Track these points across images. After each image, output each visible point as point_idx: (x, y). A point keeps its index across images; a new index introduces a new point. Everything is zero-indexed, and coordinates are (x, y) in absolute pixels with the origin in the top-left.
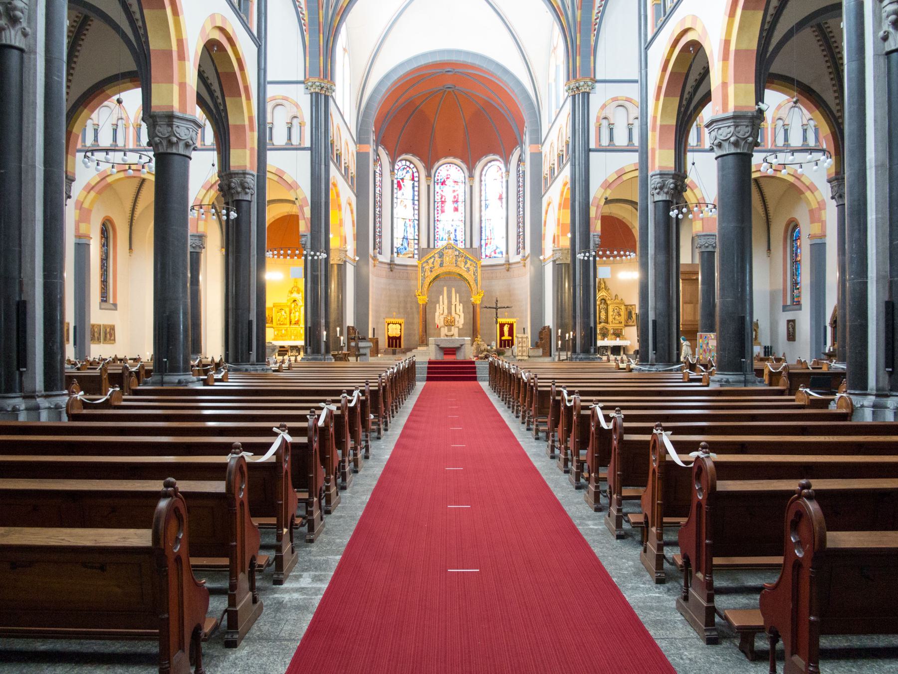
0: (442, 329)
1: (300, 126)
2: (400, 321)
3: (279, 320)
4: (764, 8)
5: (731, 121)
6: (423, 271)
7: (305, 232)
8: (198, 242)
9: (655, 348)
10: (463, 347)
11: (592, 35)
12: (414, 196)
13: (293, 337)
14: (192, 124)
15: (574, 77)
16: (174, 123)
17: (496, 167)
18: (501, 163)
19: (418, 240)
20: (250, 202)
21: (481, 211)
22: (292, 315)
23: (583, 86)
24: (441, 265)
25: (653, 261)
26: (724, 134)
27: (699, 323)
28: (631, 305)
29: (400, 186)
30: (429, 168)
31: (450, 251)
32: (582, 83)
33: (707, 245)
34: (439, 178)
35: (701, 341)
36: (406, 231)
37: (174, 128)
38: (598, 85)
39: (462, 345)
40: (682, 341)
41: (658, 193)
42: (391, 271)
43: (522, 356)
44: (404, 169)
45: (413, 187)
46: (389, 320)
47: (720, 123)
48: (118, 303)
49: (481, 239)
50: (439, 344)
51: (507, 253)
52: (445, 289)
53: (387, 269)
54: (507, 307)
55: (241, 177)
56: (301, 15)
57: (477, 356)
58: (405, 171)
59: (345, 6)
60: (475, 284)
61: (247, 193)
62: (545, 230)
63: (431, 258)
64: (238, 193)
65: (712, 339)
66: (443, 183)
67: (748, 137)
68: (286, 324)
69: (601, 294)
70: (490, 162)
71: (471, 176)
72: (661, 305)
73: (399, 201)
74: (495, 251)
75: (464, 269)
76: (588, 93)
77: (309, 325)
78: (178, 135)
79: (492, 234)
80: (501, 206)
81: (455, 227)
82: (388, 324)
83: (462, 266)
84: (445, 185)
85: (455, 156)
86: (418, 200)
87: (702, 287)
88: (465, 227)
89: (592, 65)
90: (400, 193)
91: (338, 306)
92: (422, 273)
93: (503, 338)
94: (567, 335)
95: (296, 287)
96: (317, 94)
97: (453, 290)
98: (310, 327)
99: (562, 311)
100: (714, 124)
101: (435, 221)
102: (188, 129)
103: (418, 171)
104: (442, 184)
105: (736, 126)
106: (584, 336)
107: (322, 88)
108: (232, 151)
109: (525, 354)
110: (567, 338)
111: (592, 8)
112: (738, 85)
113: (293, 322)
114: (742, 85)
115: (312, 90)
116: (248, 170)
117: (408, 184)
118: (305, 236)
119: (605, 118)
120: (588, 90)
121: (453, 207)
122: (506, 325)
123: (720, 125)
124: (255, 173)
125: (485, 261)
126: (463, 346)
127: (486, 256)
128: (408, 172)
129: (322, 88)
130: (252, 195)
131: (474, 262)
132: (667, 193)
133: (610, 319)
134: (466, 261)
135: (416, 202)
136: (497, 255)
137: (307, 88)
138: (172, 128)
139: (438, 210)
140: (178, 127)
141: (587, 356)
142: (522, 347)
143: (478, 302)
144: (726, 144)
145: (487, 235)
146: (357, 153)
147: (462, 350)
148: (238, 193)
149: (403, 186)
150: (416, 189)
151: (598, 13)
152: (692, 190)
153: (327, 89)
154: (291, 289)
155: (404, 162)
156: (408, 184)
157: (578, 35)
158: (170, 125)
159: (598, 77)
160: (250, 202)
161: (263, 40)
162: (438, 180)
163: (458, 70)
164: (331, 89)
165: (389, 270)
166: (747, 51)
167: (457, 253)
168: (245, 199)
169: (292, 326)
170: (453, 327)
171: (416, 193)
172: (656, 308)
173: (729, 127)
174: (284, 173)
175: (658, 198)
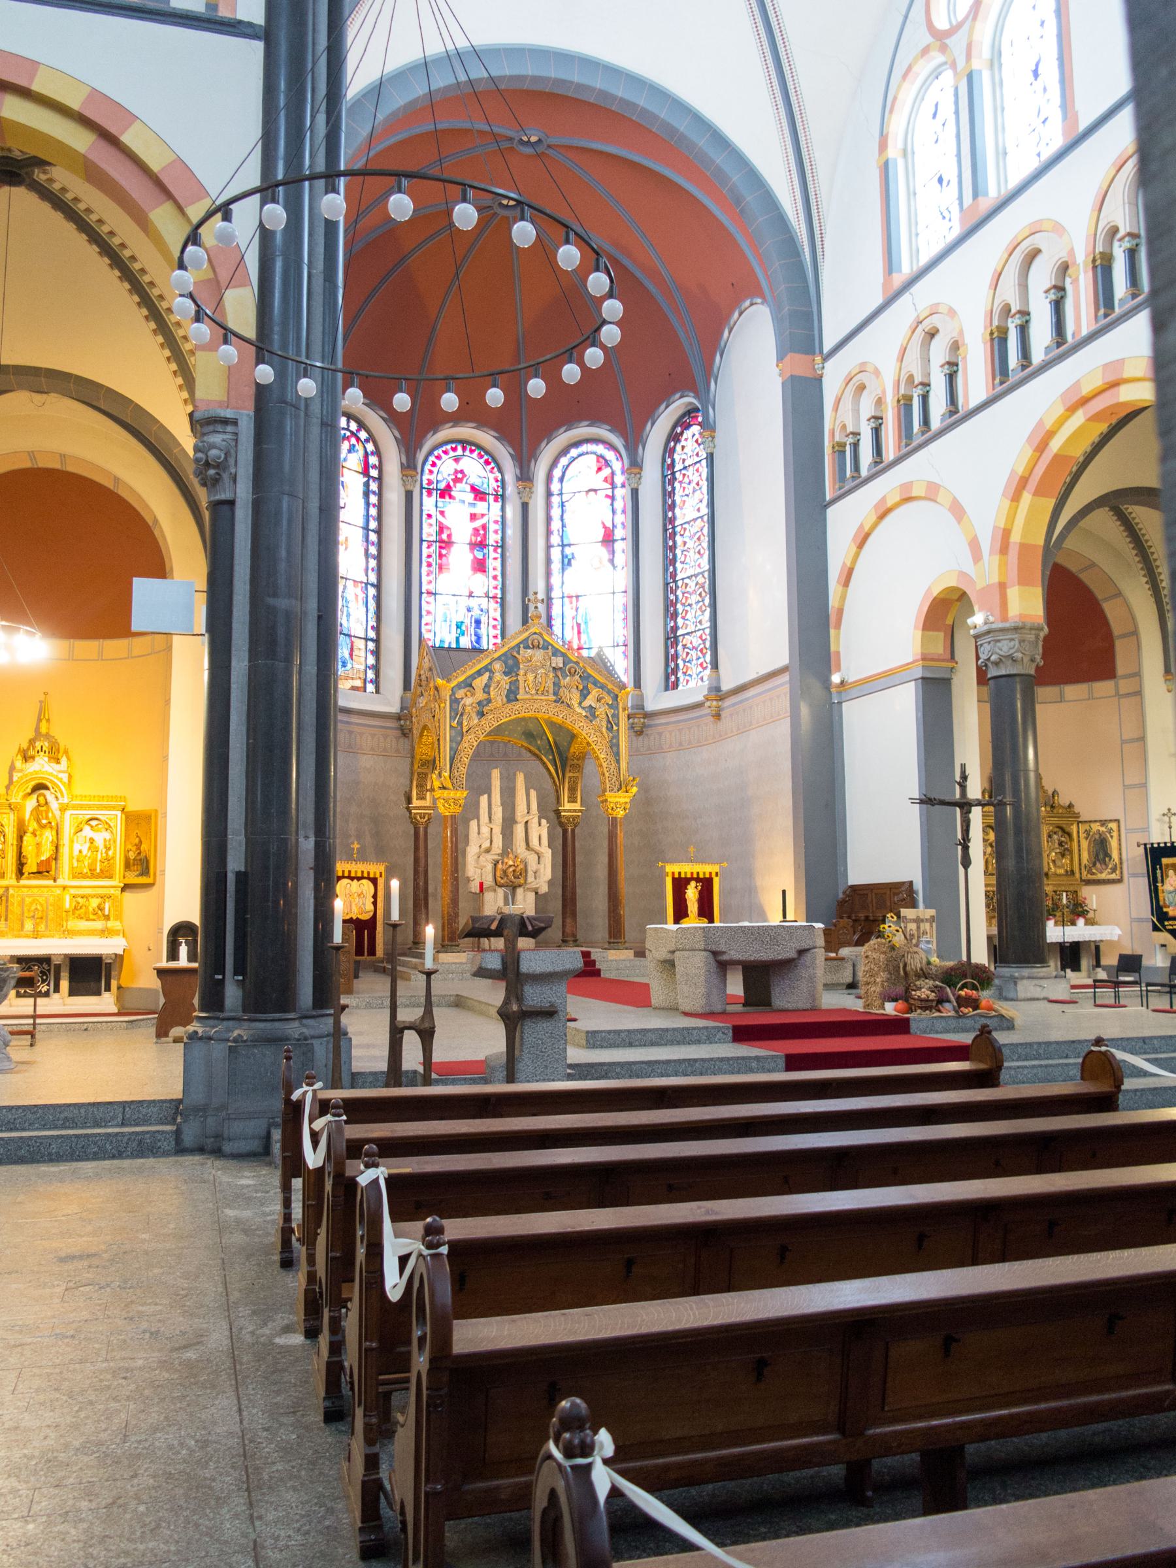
12: (367, 517)
13: (29, 926)
17: (594, 457)
18: (611, 446)
19: (377, 641)
21: (548, 574)
22: (28, 838)
24: (512, 695)
28: (1103, 823)
31: (538, 655)
39: (802, 952)
45: (366, 494)
50: (722, 948)
52: (496, 774)
60: (611, 758)
62: (843, 598)
63: (479, 673)
66: (446, 493)
70: (577, 444)
75: (579, 710)
77: (235, 862)
79: (583, 636)
80: (612, 561)
81: (476, 613)
84: (451, 497)
86: (379, 532)
88: (503, 615)
92: (452, 718)
95: (47, 736)
97: (520, 780)
98: (238, 874)
101: (421, 593)
104: (442, 496)
118: (225, 422)
121: (471, 557)
122: (693, 883)
126: (808, 957)
135: (373, 537)
143: (621, 813)
154: (25, 745)
162: (430, 482)
167: (558, 662)
169: (23, 882)
171: (373, 511)
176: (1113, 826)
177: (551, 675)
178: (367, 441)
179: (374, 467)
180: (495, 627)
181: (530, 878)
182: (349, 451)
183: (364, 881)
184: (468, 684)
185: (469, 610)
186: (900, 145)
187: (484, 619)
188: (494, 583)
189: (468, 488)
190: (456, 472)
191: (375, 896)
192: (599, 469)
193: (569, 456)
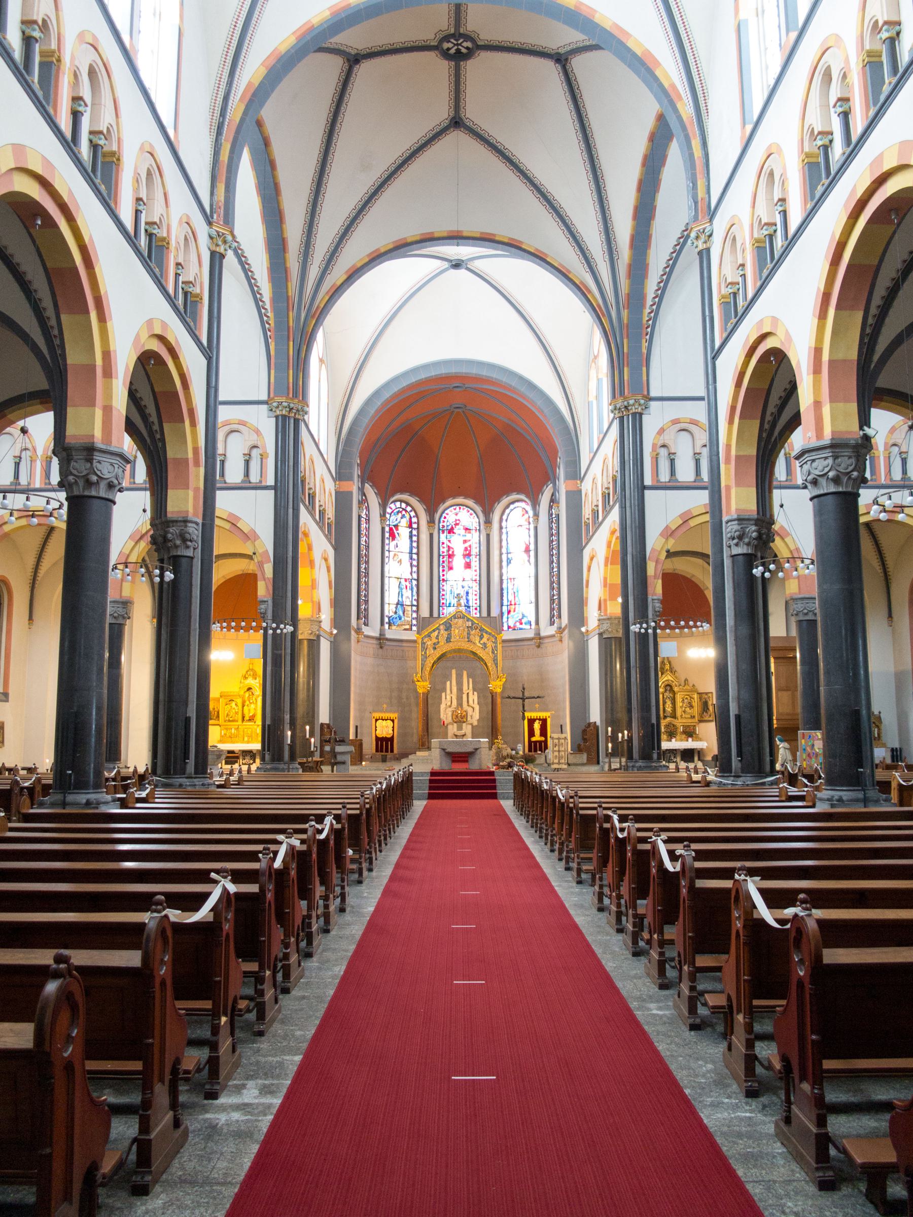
0: (450, 727)
1: (262, 459)
2: (393, 716)
3: (228, 715)
4: (863, 308)
5: (828, 451)
6: (424, 648)
7: (265, 596)
8: (121, 611)
9: (740, 753)
10: (478, 751)
11: (644, 341)
12: (411, 548)
13: (246, 739)
14: (118, 459)
15: (622, 393)
16: (95, 457)
18: (528, 504)
19: (418, 606)
20: (192, 558)
21: (501, 567)
22: (245, 708)
23: (634, 405)
24: (448, 640)
25: (733, 634)
26: (820, 468)
27: (800, 717)
28: (707, 694)
29: (393, 536)
30: (431, 511)
31: (460, 621)
32: (631, 402)
33: (806, 611)
34: (445, 524)
35: (803, 741)
36: (400, 594)
37: (95, 464)
38: (653, 404)
39: (476, 749)
40: (778, 743)
41: (737, 545)
42: (381, 647)
43: (559, 763)
44: (398, 512)
45: (411, 537)
46: (377, 715)
47: (814, 453)
48: (11, 691)
49: (502, 605)
50: (445, 747)
51: (537, 623)
52: (454, 672)
53: (375, 646)
54: (538, 697)
55: (182, 526)
56: (265, 318)
57: (498, 765)
58: (400, 515)
59: (322, 306)
60: (494, 666)
61: (188, 547)
62: (587, 593)
63: (434, 631)
64: (176, 547)
65: (819, 739)
66: (451, 531)
67: (852, 471)
68: (237, 721)
69: (666, 678)
70: (513, 503)
71: (488, 522)
72: (746, 695)
73: (392, 554)
74: (521, 620)
76: (641, 414)
77: (268, 722)
78: (99, 473)
80: (529, 561)
81: (466, 589)
82: (376, 720)
83: (477, 642)
84: (453, 533)
85: (466, 496)
86: (418, 554)
87: (801, 669)
88: (480, 589)
89: (645, 378)
90: (393, 544)
91: (308, 696)
92: (422, 651)
93: (533, 739)
94: (620, 735)
95: (252, 670)
96: (284, 417)
97: (465, 673)
99: (612, 702)
100: (806, 456)
101: (439, 581)
102: (112, 464)
103: (417, 516)
104: (449, 533)
105: (835, 457)
106: (643, 736)
107: (291, 409)
108: (170, 492)
109: (563, 761)
110: (620, 740)
111: (642, 305)
112: (834, 405)
113: (247, 718)
114: (841, 405)
115: (278, 413)
116: (191, 517)
117: (404, 532)
118: (265, 601)
119: (664, 446)
120: (640, 410)
121: (464, 561)
122: (537, 721)
123: (814, 456)
124: (200, 521)
125: (507, 635)
126: (478, 751)
127: (509, 627)
128: (403, 517)
129: (291, 409)
130: (194, 549)
131: (493, 636)
132: (748, 544)
133: (679, 712)
134: (482, 635)
135: (415, 557)
136: (523, 626)
137: (271, 410)
138: (92, 464)
139: (443, 567)
140: (99, 462)
141: (649, 764)
142: (559, 751)
143: (499, 690)
144: (823, 481)
145: (510, 600)
146: (336, 492)
147: (477, 756)
148: (176, 547)
149: (396, 535)
150: (415, 538)
151: (650, 313)
152: (783, 539)
153: (298, 410)
154: (245, 673)
155: (398, 504)
156: (404, 532)
157: (625, 341)
158: (90, 460)
159: (653, 394)
160: (192, 558)
161: (215, 350)
162: (443, 526)
163: (470, 386)
164: (303, 411)
165: (378, 647)
166: (845, 361)
167: (470, 624)
168: (185, 554)
170: (464, 725)
171: (415, 544)
172: (739, 699)
173: (826, 458)
174: (239, 519)
175: (736, 551)
176: (710, 695)
177: (466, 630)
178: (411, 511)
179: (415, 523)
180: (476, 595)
181: (469, 719)
182: (402, 518)
183: (389, 721)
184: (429, 636)
185: (463, 587)
186: (595, 394)
187: (470, 591)
188: (476, 573)
189: (462, 528)
190: (456, 520)
191: (393, 727)
192: (523, 515)
193: (510, 509)
